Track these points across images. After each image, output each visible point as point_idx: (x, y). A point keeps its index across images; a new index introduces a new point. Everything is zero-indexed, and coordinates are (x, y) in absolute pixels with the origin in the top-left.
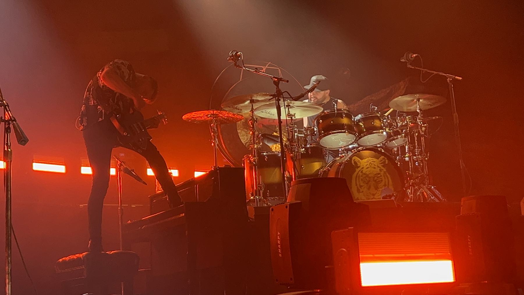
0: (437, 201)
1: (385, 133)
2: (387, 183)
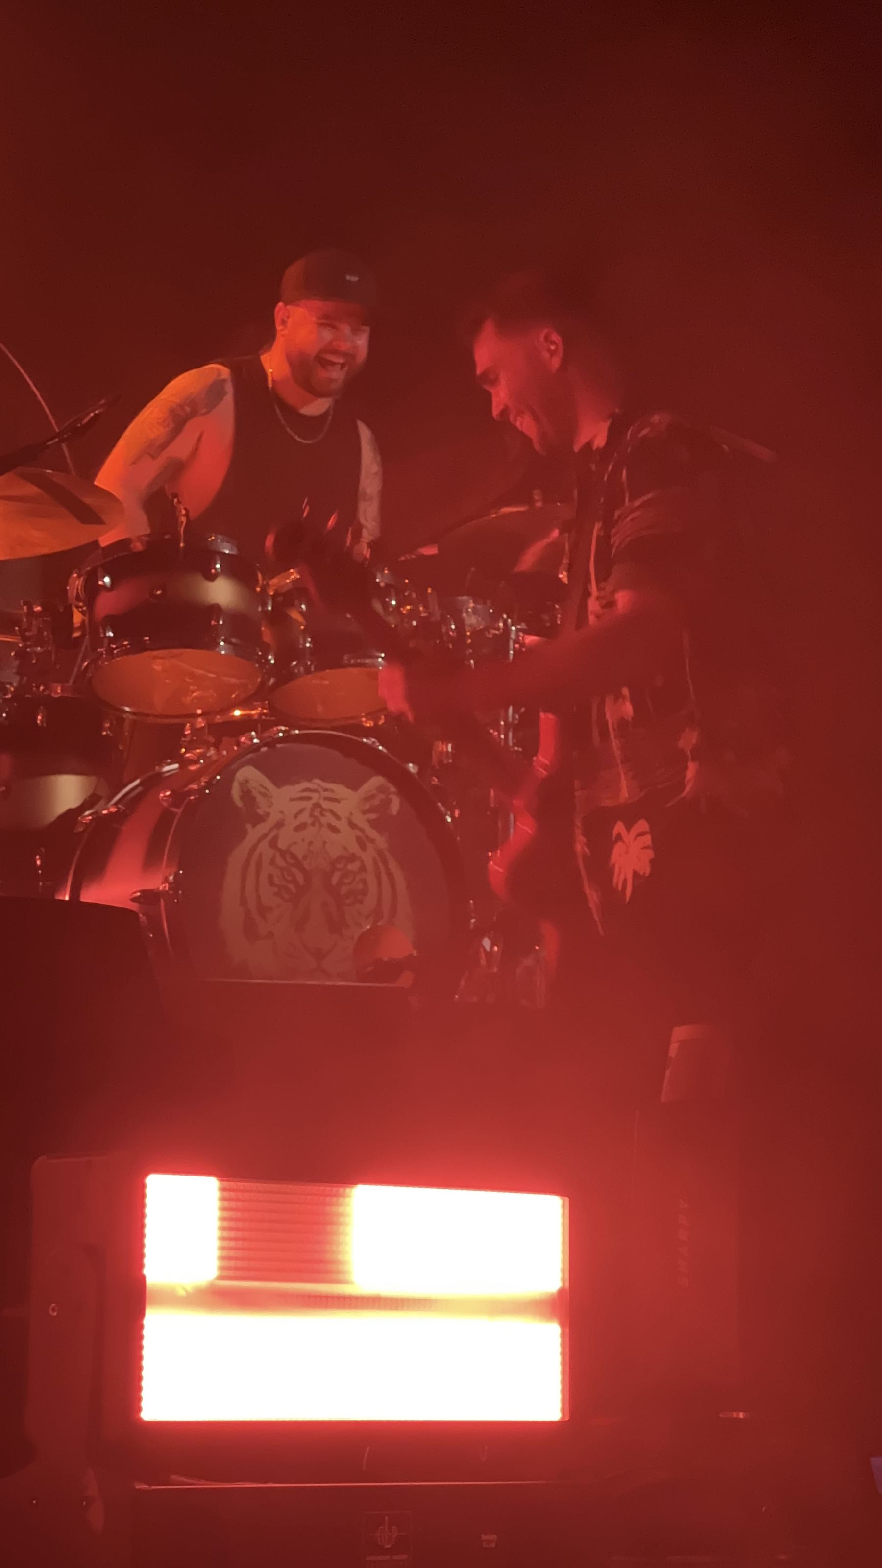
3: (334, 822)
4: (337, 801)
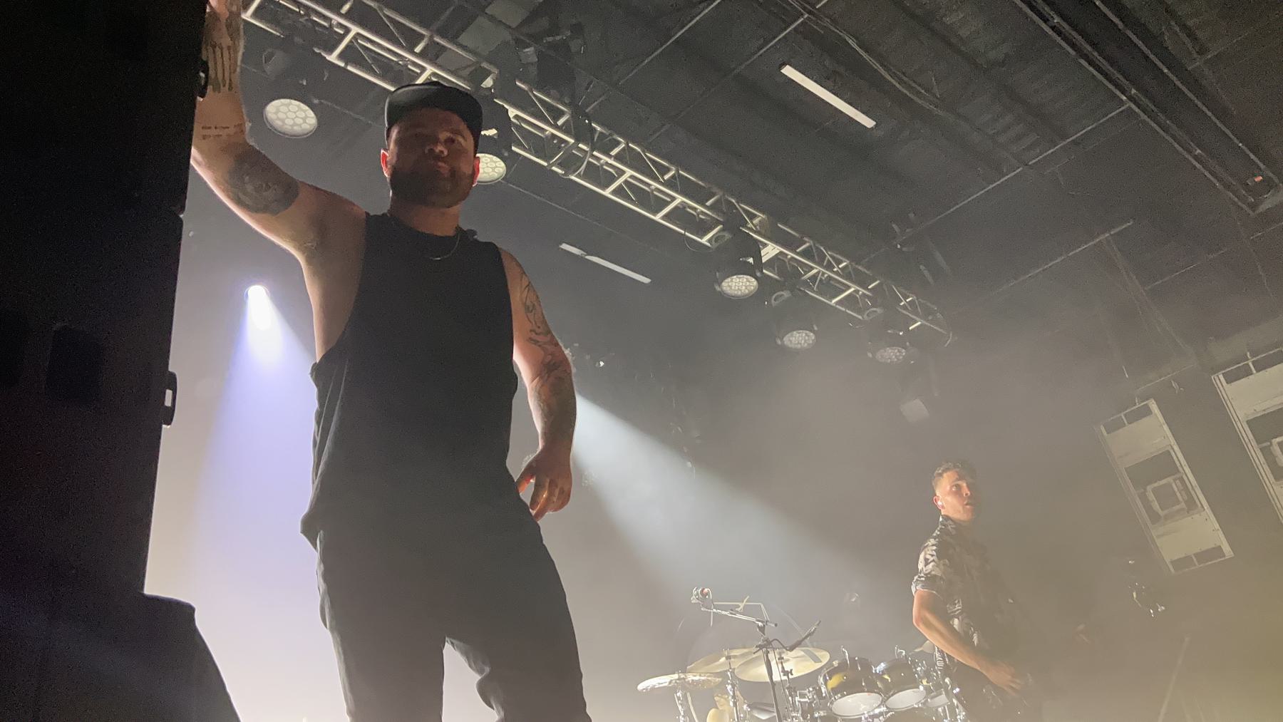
1: (921, 688)
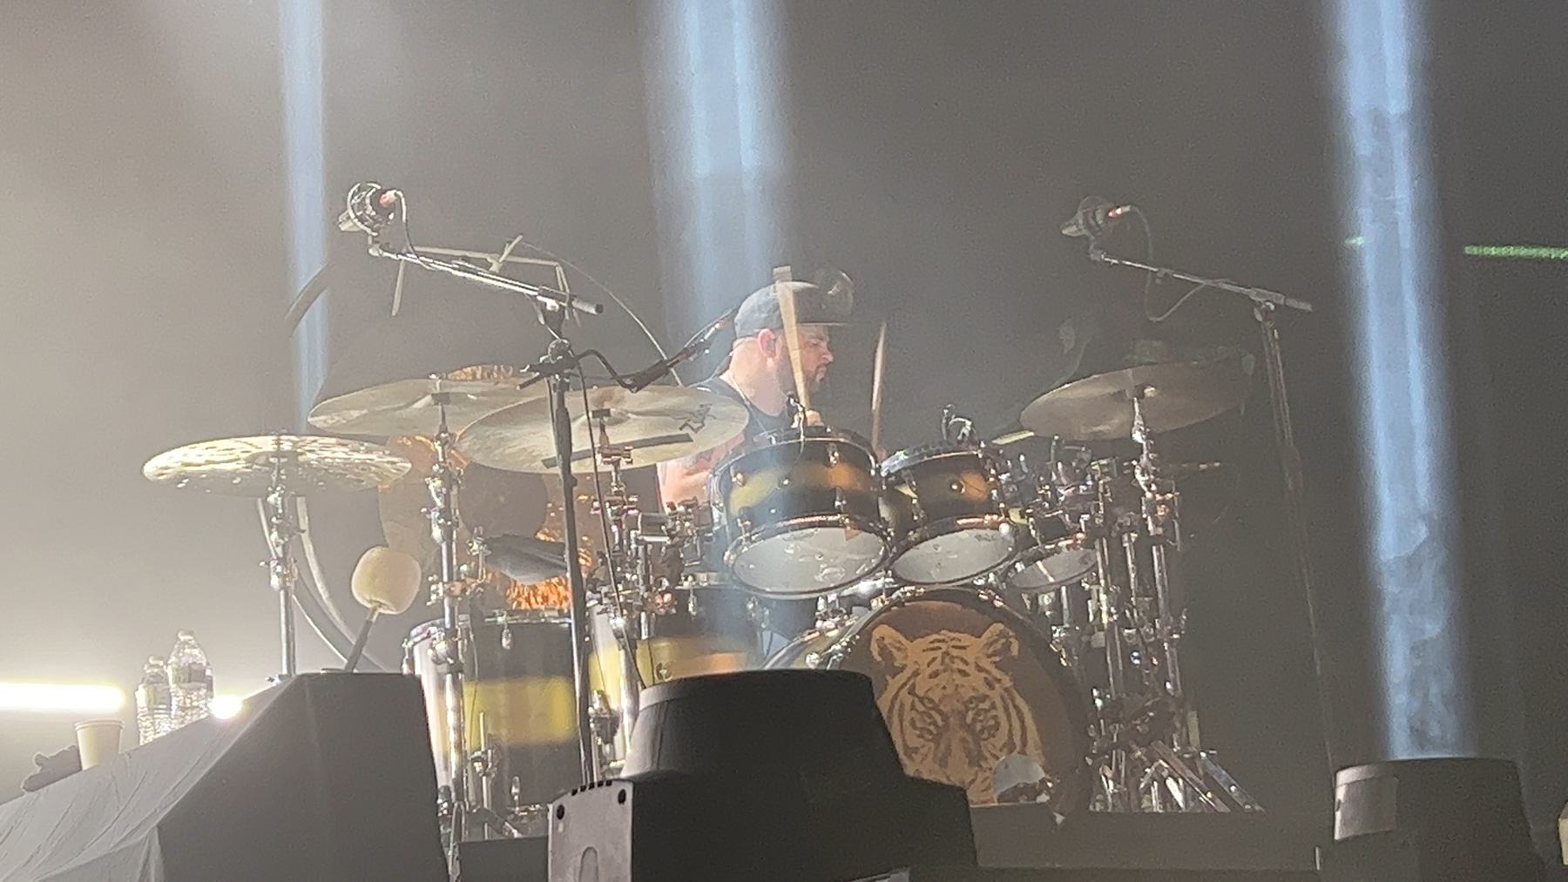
0: (1223, 808)
1: (1004, 528)
2: (1017, 740)
3: (962, 667)
4: (964, 648)
